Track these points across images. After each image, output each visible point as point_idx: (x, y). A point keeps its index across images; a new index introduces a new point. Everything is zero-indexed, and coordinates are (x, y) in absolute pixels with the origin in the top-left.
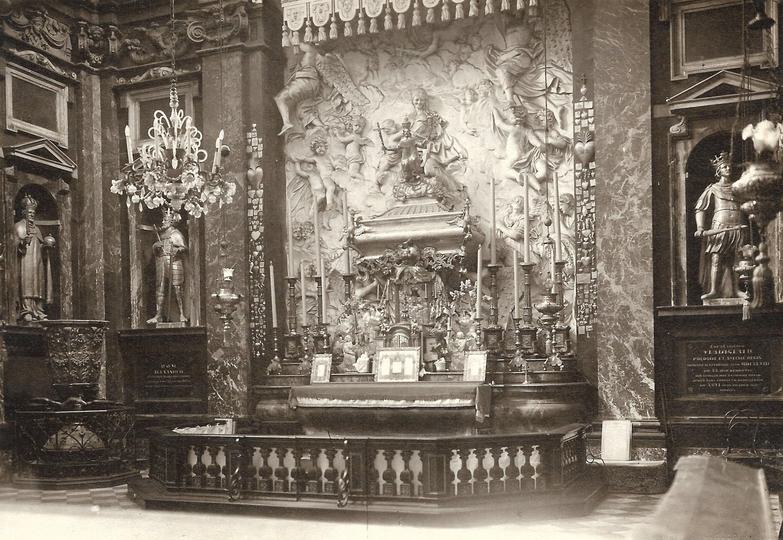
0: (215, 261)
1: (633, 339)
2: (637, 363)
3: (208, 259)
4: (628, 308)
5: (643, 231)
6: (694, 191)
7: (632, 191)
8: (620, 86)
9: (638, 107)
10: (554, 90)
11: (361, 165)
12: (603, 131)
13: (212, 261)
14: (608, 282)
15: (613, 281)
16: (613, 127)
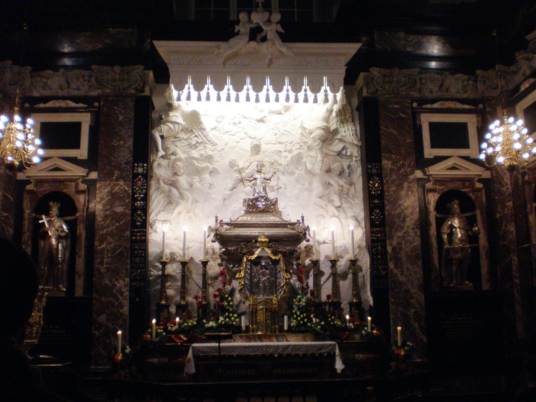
0: (104, 245)
1: (413, 310)
2: (416, 325)
3: (97, 243)
4: (409, 290)
5: (415, 244)
6: (440, 222)
7: (408, 219)
8: (398, 157)
9: (408, 170)
10: (344, 152)
11: (211, 185)
12: (390, 182)
13: (100, 245)
14: (396, 274)
15: (399, 274)
16: (395, 180)
